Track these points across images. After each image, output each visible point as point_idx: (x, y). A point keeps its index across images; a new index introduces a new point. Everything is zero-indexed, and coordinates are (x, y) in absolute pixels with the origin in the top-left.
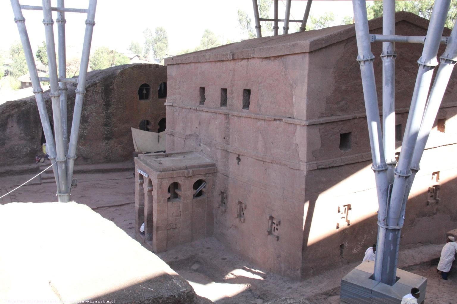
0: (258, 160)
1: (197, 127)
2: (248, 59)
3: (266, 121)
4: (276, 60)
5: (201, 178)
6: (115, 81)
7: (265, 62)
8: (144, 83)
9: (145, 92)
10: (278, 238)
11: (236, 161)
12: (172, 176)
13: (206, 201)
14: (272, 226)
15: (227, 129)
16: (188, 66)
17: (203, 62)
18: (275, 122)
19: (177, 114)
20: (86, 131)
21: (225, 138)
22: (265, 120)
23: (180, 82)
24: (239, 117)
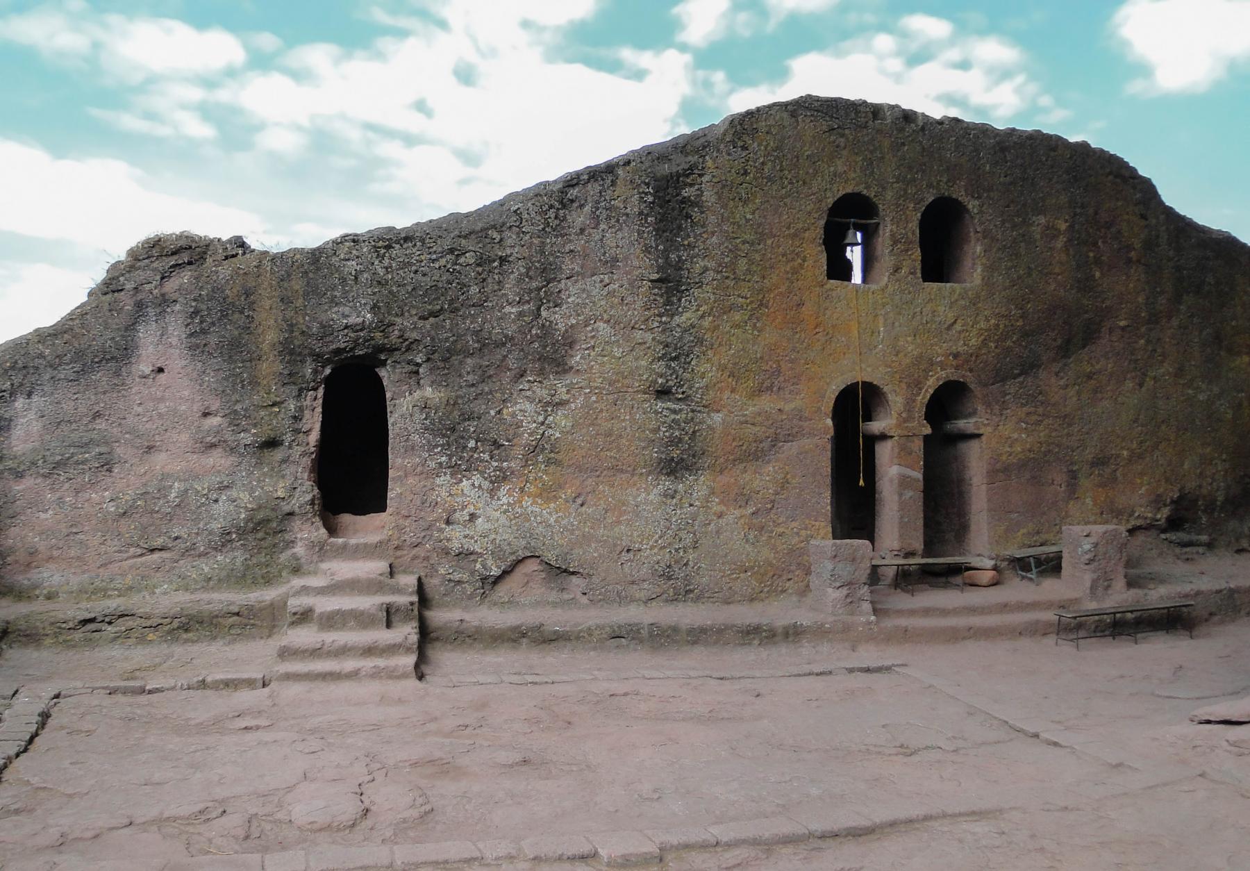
6: (710, 163)
20: (561, 419)
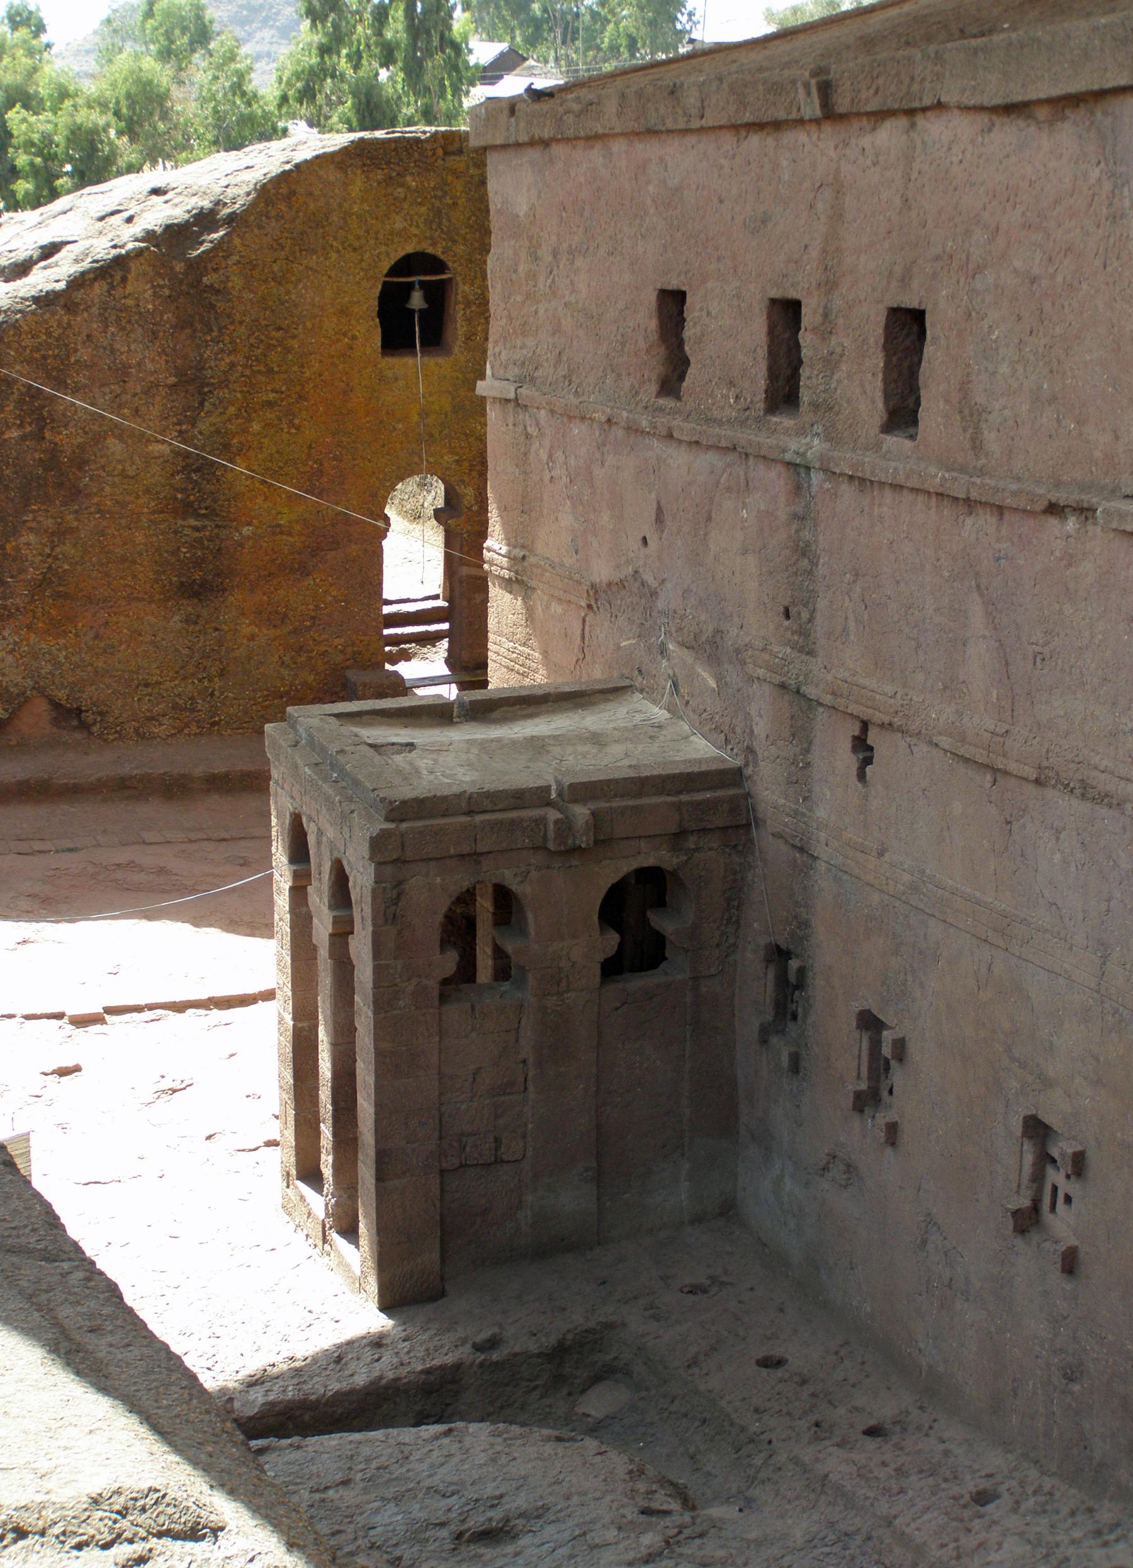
0: (967, 760)
1: (645, 541)
2: (911, 112)
3: (1007, 514)
4: (1067, 125)
5: (649, 861)
7: (1007, 132)
8: (410, 249)
9: (417, 301)
10: (1070, 1263)
11: (847, 760)
12: (466, 849)
13: (688, 999)
14: (1038, 1177)
15: (804, 555)
16: (596, 155)
17: (669, 131)
18: (1053, 521)
19: (544, 456)
21: (793, 611)
22: (1000, 510)
23: (555, 254)
24: (861, 482)
